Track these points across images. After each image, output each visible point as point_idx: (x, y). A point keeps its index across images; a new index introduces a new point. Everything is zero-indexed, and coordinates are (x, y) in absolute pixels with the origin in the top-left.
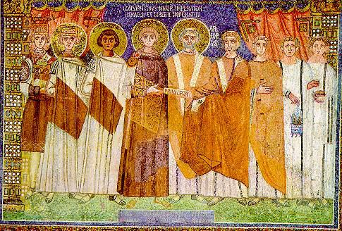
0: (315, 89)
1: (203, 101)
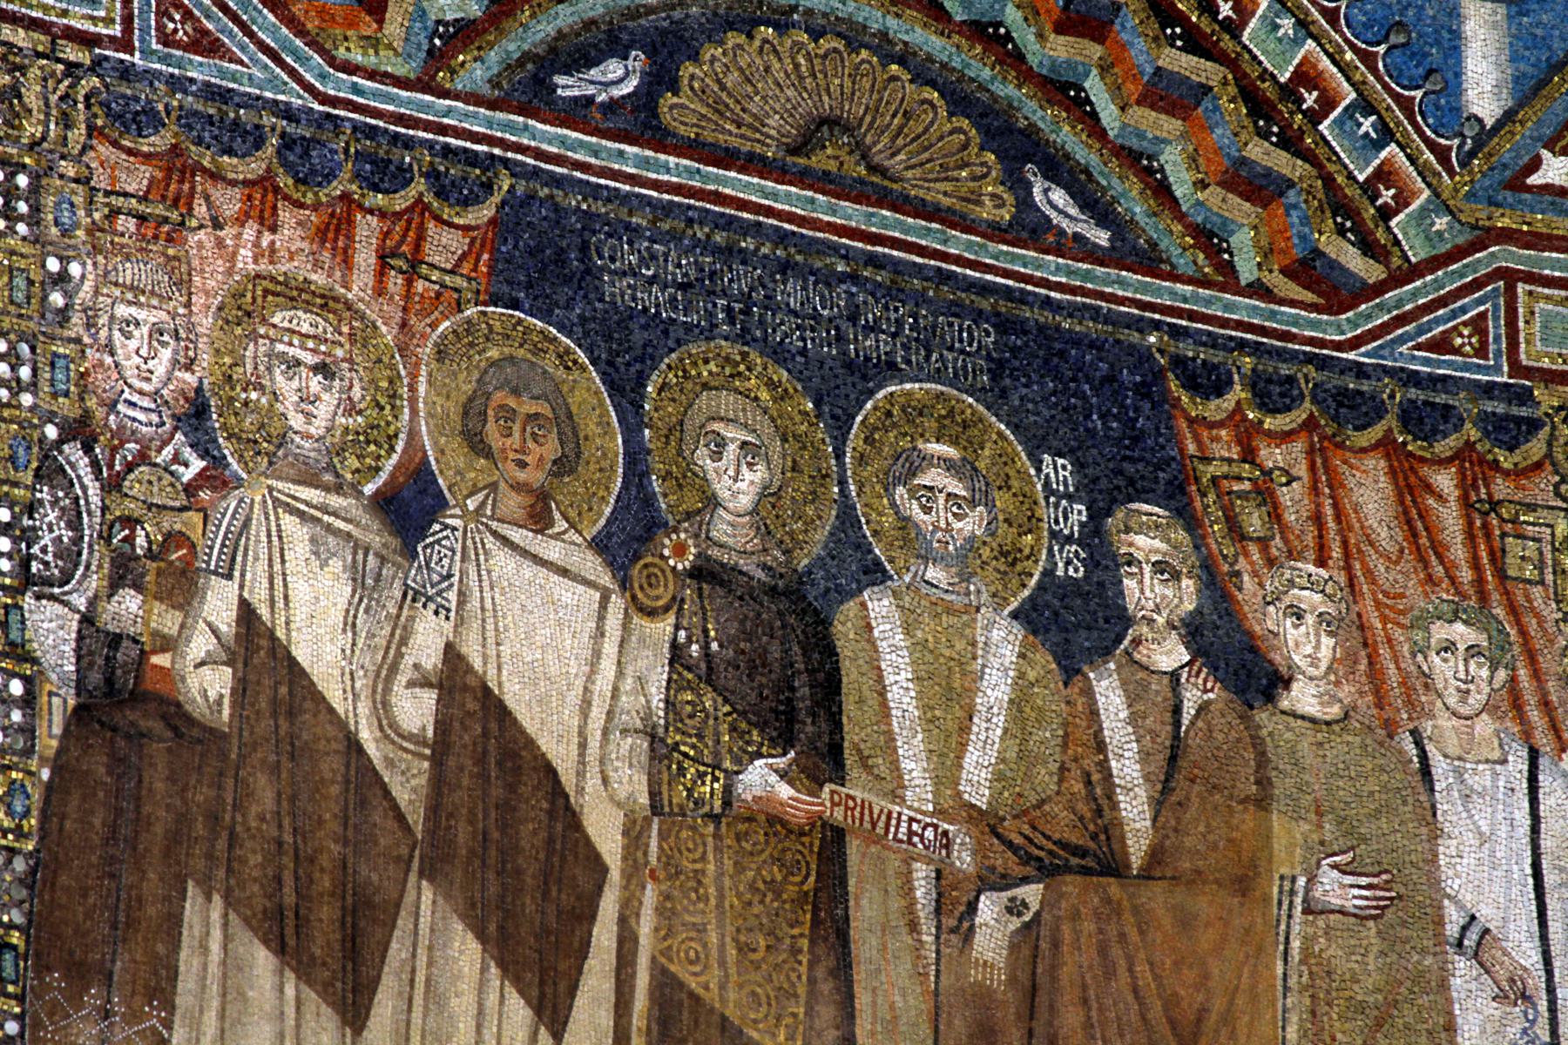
1: (1035, 907)
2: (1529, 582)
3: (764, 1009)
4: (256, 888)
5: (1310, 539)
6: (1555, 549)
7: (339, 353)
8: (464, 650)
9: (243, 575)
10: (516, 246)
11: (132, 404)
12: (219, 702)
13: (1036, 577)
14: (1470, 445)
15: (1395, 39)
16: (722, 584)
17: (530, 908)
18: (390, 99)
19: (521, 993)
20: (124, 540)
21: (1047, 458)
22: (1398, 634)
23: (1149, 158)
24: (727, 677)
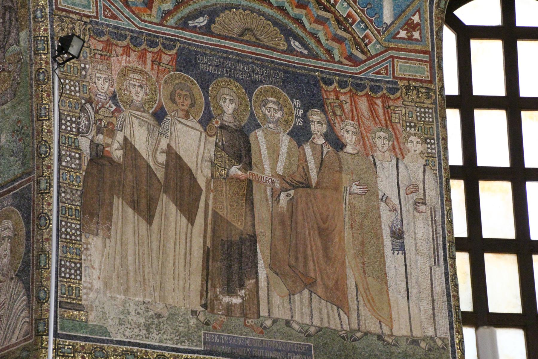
1: (292, 195)
2: (397, 123)
3: (236, 218)
4: (129, 196)
5: (350, 115)
6: (402, 116)
7: (144, 83)
8: (171, 145)
9: (124, 131)
10: (181, 59)
12: (120, 158)
13: (292, 125)
14: (384, 94)
15: (368, 7)
16: (226, 129)
17: (186, 199)
18: (154, 28)
19: (185, 216)
20: (99, 124)
21: (295, 100)
23: (316, 34)
24: (227, 149)
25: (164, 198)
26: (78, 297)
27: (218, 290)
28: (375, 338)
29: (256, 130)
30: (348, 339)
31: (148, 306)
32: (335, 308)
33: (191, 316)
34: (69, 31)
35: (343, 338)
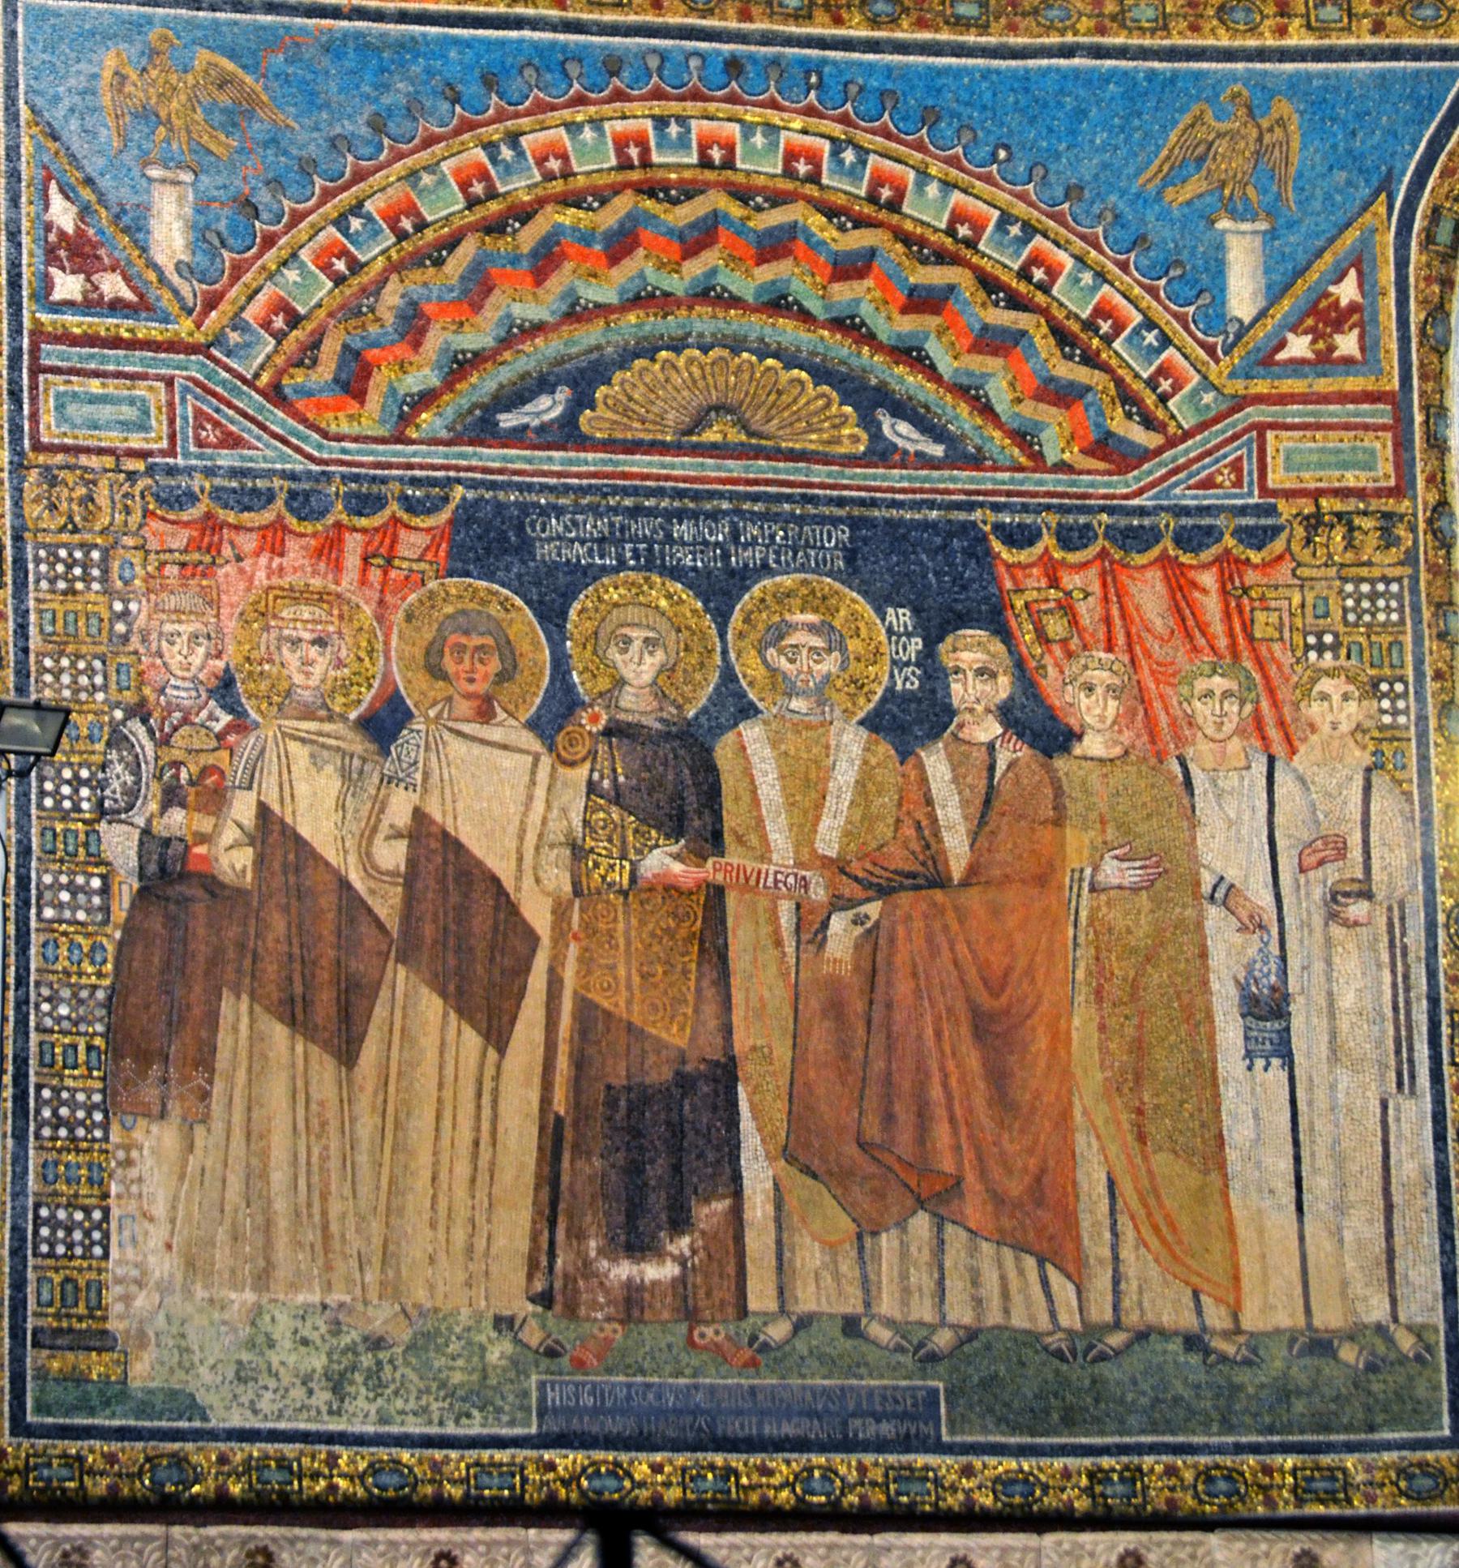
0: (1332, 873)
1: (875, 916)
4: (273, 987)
5: (1101, 634)
6: (1291, 614)
7: (331, 629)
8: (427, 810)
11: (177, 688)
12: (244, 871)
21: (890, 610)
22: (1169, 691)
25: (400, 976)
26: (97, 1309)
27: (593, 1244)
28: (1175, 1346)
29: (741, 726)
30: (1075, 1357)
31: (341, 1317)
32: (1030, 1262)
33: (494, 1335)
34: (75, 507)
35: (1059, 1354)
